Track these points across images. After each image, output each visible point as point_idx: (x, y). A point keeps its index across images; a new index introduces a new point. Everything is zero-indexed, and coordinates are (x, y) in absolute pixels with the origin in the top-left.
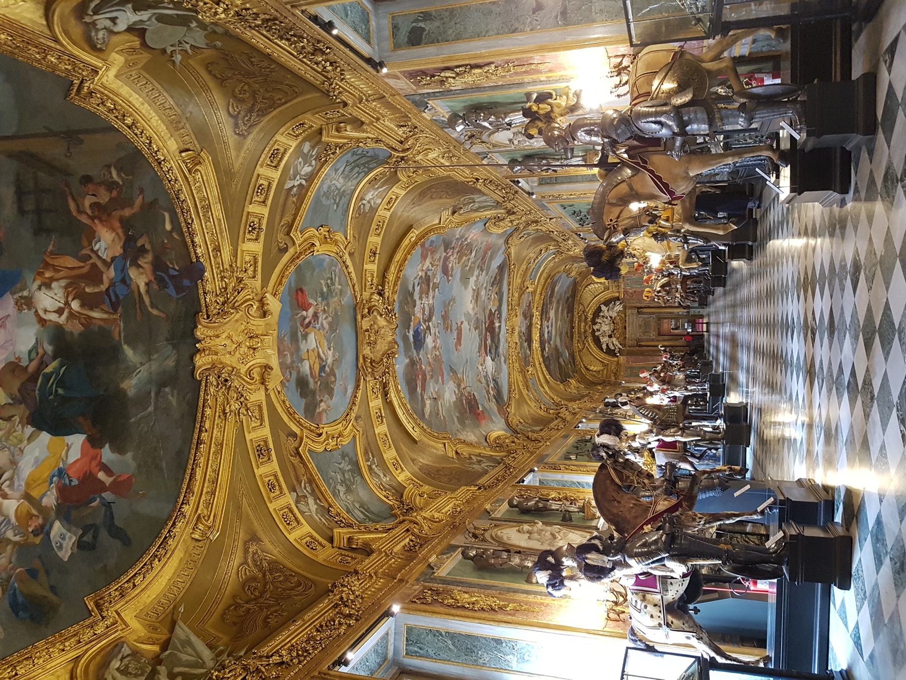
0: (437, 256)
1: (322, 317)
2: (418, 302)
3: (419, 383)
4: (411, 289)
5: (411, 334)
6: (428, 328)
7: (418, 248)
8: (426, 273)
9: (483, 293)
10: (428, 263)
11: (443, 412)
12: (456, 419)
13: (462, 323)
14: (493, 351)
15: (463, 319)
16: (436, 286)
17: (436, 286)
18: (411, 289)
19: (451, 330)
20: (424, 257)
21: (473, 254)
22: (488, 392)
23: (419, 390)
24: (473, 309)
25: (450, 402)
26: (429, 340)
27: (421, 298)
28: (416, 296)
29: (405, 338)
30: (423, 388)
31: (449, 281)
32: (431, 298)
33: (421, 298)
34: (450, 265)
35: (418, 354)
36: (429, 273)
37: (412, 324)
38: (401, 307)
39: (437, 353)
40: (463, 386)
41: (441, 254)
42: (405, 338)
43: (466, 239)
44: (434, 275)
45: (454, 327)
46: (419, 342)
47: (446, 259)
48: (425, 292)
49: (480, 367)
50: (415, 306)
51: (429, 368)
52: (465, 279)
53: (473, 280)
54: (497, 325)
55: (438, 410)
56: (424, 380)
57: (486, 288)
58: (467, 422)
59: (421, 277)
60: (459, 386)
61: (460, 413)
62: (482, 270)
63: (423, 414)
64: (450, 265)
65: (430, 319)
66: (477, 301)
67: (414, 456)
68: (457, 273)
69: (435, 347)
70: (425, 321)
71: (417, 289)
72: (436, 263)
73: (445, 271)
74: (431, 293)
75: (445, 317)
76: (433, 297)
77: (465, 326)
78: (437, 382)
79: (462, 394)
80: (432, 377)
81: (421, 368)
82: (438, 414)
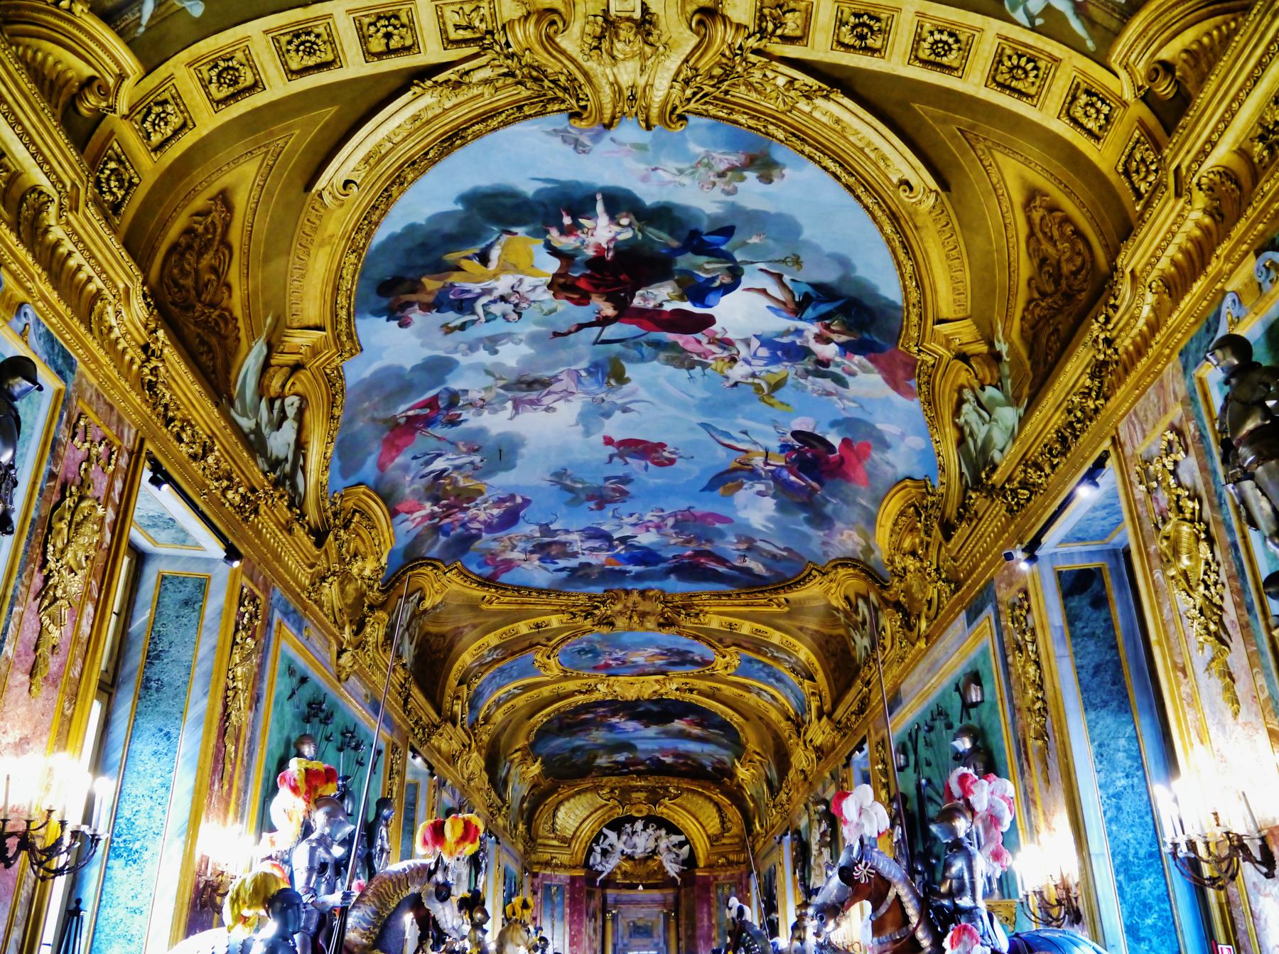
0: (495, 546)
1: (615, 656)
2: (583, 559)
3: (712, 565)
4: (564, 574)
5: (634, 569)
6: (623, 540)
7: (504, 578)
8: (532, 552)
9: (512, 356)
10: (516, 555)
11: (775, 546)
12: (806, 528)
13: (608, 441)
14: (706, 268)
15: (598, 439)
16: (545, 529)
17: (545, 529)
18: (564, 574)
19: (626, 480)
20: (509, 565)
21: (439, 464)
22: (821, 367)
23: (721, 569)
24: (567, 395)
25: (769, 519)
26: (647, 539)
27: (574, 555)
28: (573, 563)
29: (639, 577)
30: (722, 561)
31: (526, 502)
32: (570, 537)
33: (574, 555)
34: (496, 512)
35: (665, 560)
36: (530, 547)
37: (617, 568)
38: (595, 583)
39: (671, 522)
40: (758, 461)
41: (487, 541)
42: (639, 577)
43: (432, 515)
44: (529, 538)
45: (618, 469)
46: (647, 556)
47: (489, 527)
48: (565, 550)
49: (739, 371)
50: (589, 565)
51: (693, 545)
52: (503, 454)
53: (497, 423)
54: (602, 232)
55: (769, 552)
56: (709, 555)
57: (492, 344)
58: (829, 509)
59: (540, 559)
60: (754, 475)
61: (804, 506)
62: (453, 398)
63: (760, 577)
64: (496, 512)
65: (607, 537)
66: (544, 384)
67: (799, 624)
68: (502, 481)
69: (658, 527)
70: (611, 547)
71: (562, 563)
72: (508, 543)
73: (511, 518)
74: (562, 537)
75: (601, 499)
76: (567, 532)
77: (618, 427)
78: (722, 535)
79: (775, 476)
80: (709, 541)
81: (689, 557)
82: (774, 556)
